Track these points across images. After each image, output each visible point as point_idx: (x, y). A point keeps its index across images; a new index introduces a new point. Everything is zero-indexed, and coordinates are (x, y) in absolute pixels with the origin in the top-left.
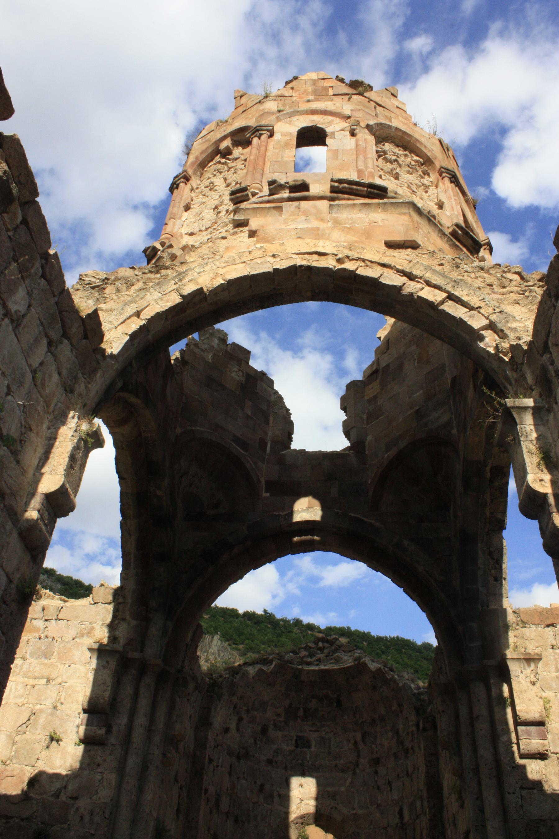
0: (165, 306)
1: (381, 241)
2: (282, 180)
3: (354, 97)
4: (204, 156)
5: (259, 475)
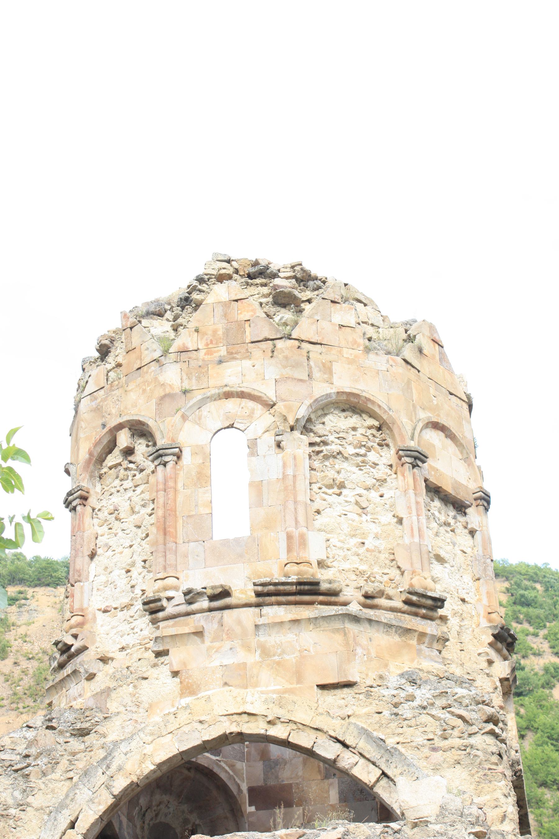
0: (99, 811)
1: (312, 687)
2: (197, 586)
3: (280, 344)
4: (99, 449)
5: (239, 782)
